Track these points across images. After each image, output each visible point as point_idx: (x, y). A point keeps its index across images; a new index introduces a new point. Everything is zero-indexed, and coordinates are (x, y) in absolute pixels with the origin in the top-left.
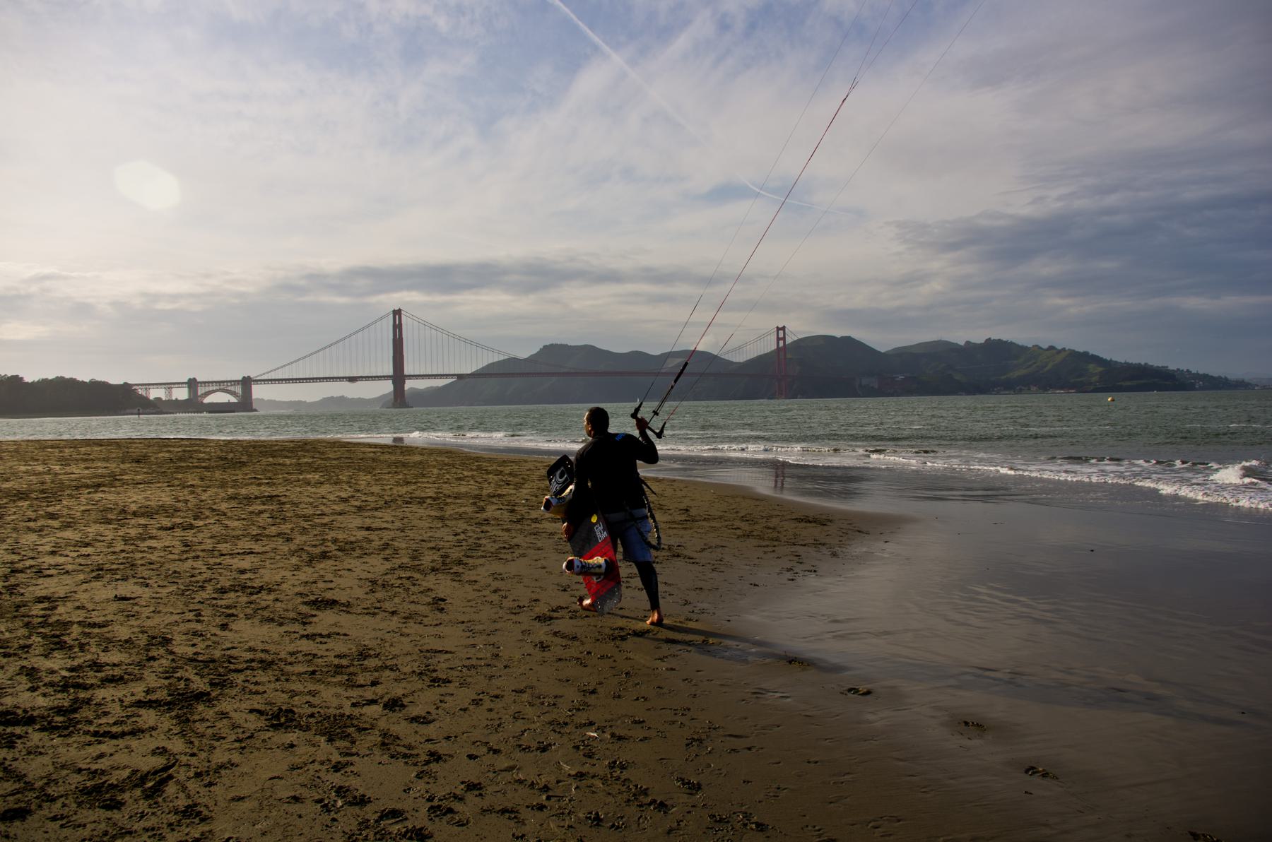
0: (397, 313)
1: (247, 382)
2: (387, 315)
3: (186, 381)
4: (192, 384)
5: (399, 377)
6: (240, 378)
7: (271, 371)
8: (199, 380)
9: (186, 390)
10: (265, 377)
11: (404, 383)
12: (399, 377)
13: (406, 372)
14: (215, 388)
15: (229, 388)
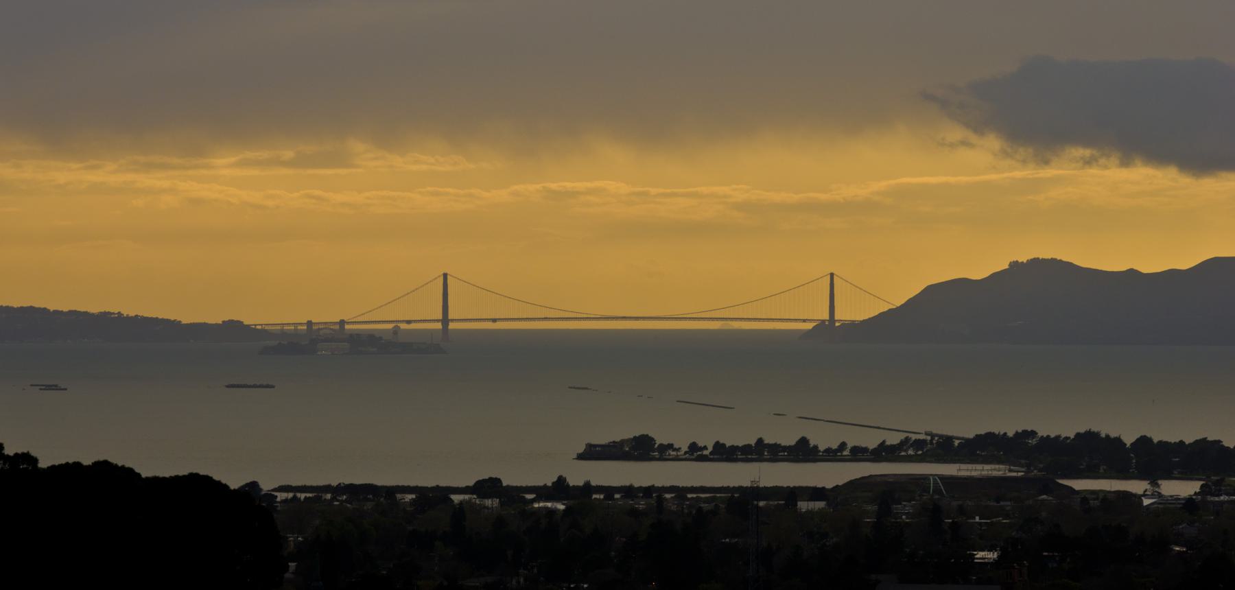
0: (445, 276)
1: (342, 322)
2: (439, 276)
3: (305, 322)
4: (310, 323)
5: (445, 320)
6: (338, 321)
7: (359, 316)
8: (313, 321)
9: (305, 327)
10: (354, 320)
11: (448, 325)
12: (445, 320)
13: (450, 318)
14: (323, 327)
15: (332, 327)
